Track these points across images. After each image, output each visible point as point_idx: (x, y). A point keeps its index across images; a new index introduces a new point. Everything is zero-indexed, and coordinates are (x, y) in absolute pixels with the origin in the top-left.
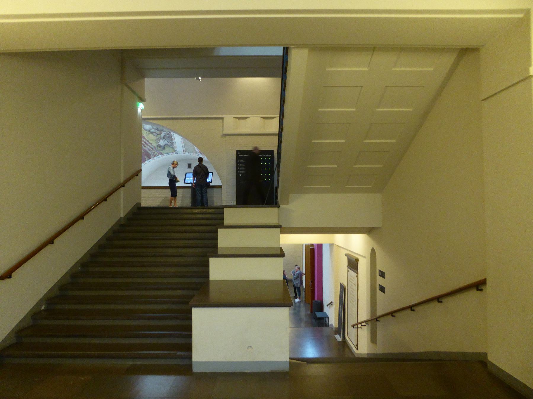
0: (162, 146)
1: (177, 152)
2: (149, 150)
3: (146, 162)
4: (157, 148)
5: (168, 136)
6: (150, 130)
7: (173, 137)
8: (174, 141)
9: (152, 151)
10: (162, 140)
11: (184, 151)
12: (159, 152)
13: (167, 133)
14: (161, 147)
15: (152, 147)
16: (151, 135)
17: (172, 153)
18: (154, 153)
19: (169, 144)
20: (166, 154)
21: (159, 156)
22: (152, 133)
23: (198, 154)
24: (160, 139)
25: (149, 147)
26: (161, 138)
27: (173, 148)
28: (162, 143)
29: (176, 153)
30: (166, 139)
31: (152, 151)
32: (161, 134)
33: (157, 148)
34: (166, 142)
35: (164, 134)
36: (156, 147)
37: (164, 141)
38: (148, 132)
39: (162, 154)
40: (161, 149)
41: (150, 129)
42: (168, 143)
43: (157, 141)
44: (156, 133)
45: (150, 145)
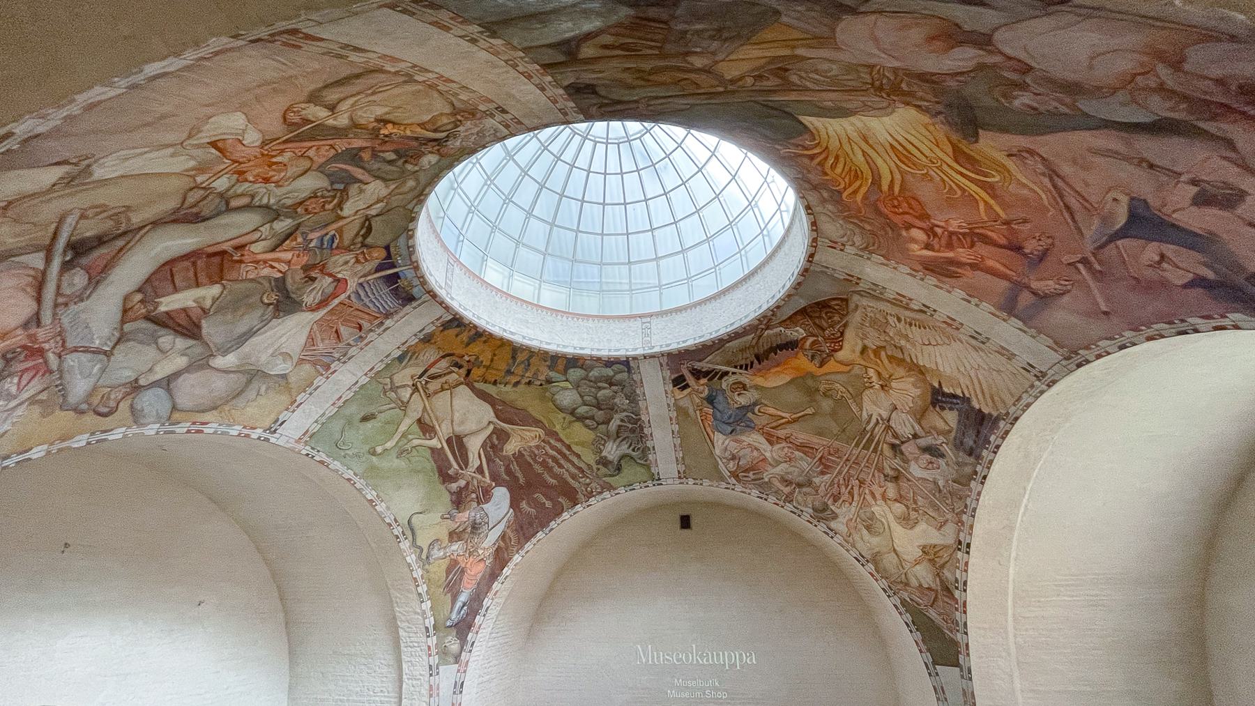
0: (611, 462)
1: (659, 479)
2: (574, 477)
3: (565, 515)
4: (598, 469)
5: (630, 426)
6: (575, 409)
7: (646, 431)
8: (649, 444)
9: (581, 480)
11: (682, 476)
12: (601, 483)
14: (610, 467)
15: (582, 465)
16: (578, 426)
17: (642, 485)
18: (588, 485)
20: (625, 486)
21: (602, 496)
22: (581, 419)
24: (605, 438)
25: (573, 470)
26: (608, 437)
27: (648, 467)
28: (612, 451)
29: (655, 482)
31: (581, 480)
32: (607, 422)
33: (598, 469)
34: (624, 449)
35: (619, 423)
36: (595, 467)
37: (617, 447)
38: (569, 418)
39: (611, 486)
42: (630, 451)
43: (597, 446)
44: (592, 418)
45: (575, 460)
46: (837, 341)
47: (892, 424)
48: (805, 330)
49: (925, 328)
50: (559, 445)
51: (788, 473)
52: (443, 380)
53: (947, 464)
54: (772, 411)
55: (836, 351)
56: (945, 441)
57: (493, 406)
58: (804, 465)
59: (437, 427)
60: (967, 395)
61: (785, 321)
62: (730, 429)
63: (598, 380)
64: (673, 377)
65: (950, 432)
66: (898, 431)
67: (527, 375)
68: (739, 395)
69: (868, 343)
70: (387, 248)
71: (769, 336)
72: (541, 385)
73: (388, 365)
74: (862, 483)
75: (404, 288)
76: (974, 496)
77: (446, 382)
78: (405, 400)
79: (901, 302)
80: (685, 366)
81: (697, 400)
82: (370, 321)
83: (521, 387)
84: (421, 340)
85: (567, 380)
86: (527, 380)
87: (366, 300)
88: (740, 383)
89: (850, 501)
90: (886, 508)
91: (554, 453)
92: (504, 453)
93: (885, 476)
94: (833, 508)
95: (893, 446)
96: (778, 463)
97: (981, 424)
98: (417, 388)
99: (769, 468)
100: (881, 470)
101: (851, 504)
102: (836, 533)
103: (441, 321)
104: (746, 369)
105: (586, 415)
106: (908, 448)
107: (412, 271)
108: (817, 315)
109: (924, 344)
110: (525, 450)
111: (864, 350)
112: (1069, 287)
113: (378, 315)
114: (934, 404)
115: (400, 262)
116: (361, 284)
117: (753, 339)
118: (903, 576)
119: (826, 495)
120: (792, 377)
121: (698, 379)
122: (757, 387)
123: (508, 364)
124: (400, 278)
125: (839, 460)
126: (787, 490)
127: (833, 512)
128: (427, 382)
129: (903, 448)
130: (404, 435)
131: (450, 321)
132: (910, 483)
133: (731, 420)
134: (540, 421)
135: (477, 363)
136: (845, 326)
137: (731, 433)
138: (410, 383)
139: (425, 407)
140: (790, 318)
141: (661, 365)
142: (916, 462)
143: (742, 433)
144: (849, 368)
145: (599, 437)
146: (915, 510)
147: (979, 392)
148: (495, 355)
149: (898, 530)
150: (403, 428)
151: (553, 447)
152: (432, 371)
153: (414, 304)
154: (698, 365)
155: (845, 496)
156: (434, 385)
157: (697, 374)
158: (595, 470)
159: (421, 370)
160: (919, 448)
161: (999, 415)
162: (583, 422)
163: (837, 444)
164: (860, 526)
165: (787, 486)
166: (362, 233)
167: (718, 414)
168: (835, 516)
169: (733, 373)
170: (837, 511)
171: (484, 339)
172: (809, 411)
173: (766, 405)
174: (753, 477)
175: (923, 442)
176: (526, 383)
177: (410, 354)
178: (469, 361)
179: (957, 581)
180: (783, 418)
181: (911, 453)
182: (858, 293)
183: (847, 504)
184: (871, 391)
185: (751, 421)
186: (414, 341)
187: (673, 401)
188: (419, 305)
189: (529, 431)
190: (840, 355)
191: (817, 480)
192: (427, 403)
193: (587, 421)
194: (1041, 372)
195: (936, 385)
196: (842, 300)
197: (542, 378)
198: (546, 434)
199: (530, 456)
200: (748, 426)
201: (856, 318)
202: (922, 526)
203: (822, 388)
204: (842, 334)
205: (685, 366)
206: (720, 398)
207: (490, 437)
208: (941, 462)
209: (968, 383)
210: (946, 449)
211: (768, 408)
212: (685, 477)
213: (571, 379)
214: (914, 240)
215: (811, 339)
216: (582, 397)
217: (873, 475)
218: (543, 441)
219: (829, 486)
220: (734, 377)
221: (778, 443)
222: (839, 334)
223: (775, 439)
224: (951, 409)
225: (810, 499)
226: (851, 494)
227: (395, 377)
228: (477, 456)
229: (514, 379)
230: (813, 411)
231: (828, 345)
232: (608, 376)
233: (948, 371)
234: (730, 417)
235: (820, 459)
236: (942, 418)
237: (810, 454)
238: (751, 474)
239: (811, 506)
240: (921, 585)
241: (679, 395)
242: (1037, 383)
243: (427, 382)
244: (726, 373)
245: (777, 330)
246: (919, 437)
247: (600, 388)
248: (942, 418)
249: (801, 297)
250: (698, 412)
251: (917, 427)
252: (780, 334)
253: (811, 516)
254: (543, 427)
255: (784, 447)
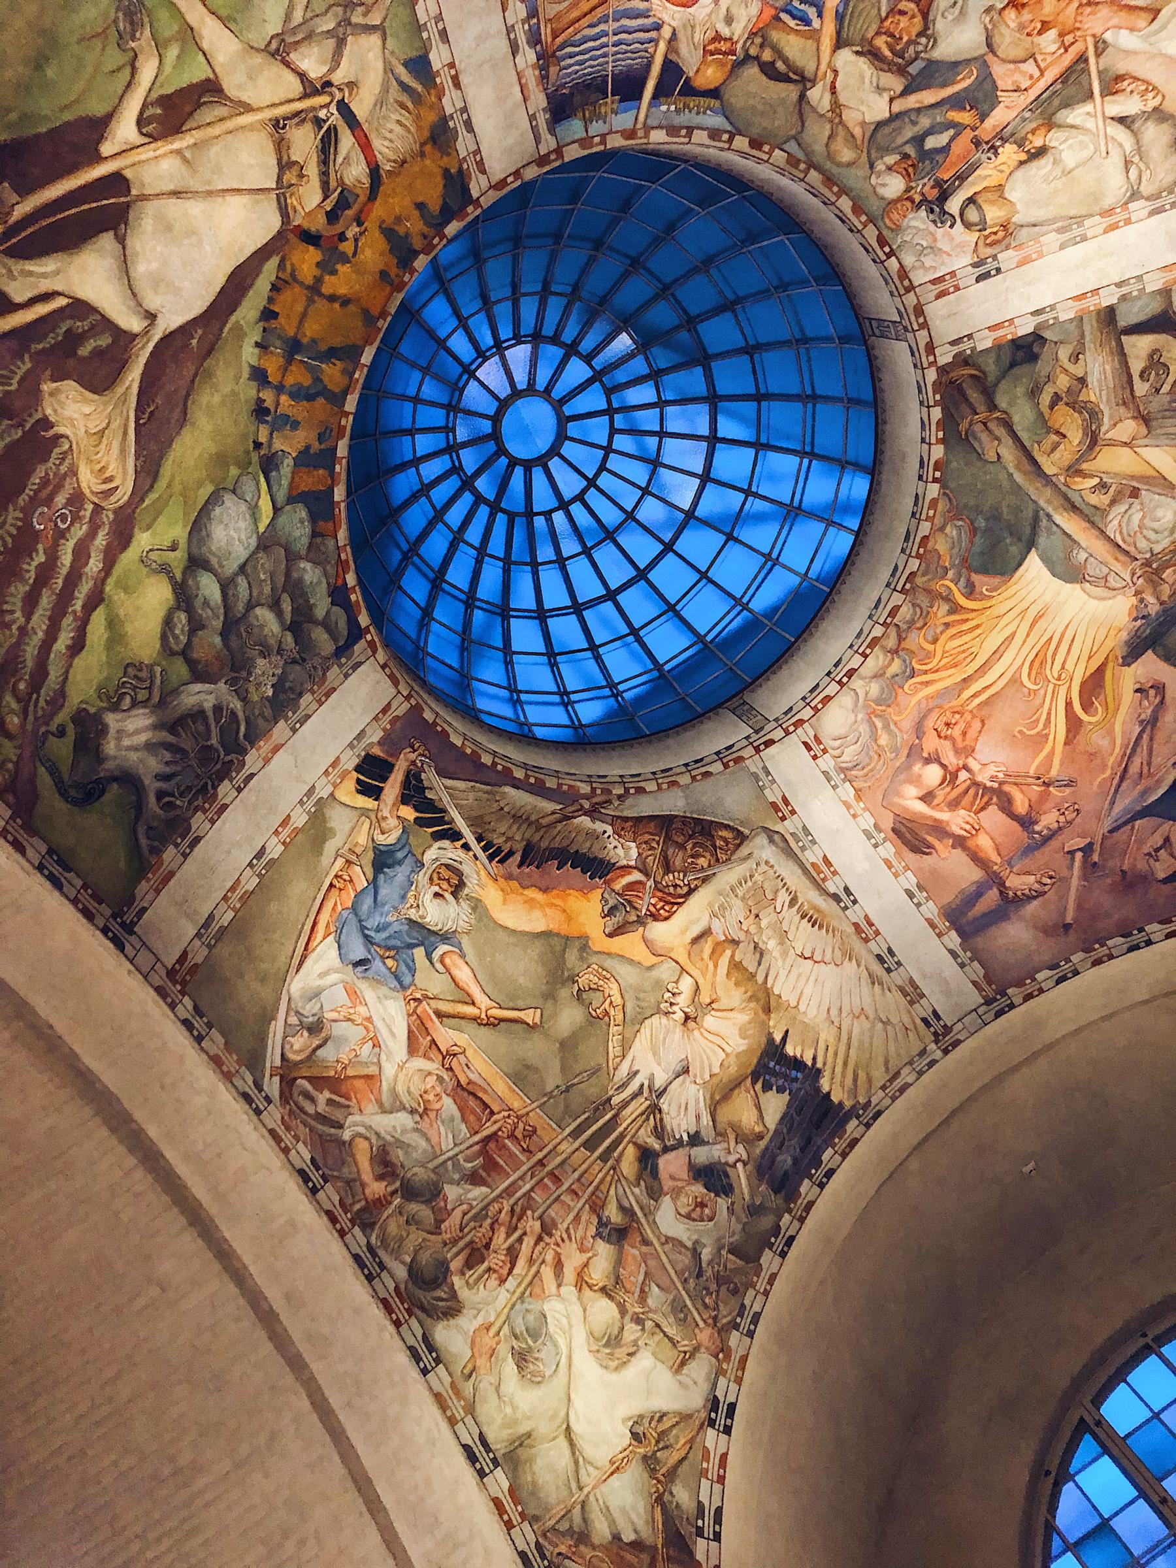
0: (100, 758)
1: (129, 928)
5: (214, 741)
6: (206, 565)
7: (225, 788)
8: (198, 821)
10: (156, 727)
13: (233, 714)
15: (54, 673)
19: (152, 799)
20: (51, 852)
22: (184, 596)
23: (259, 1086)
26: (162, 703)
29: (115, 926)
30: (168, 747)
32: (200, 674)
33: (61, 733)
34: (150, 766)
35: (209, 703)
37: (149, 747)
38: (177, 559)
40: (65, 770)
41: (214, 561)
42: (152, 786)
44: (196, 626)
46: (673, 900)
47: (664, 1104)
48: (639, 854)
49: (821, 927)
50: (94, 565)
51: (400, 1144)
52: (312, 171)
53: (731, 1210)
54: (463, 974)
55: (655, 917)
56: (745, 1157)
57: (194, 322)
58: (447, 1142)
59: (176, 145)
60: (819, 1065)
61: (626, 819)
62: (358, 951)
63: (294, 587)
64: (377, 751)
65: (760, 1137)
66: (666, 1119)
67: (284, 399)
68: (437, 895)
69: (717, 927)
70: (714, 93)
71: (579, 830)
72: (258, 445)
73: (419, 28)
74: (547, 1229)
75: (594, 103)
76: (761, 1285)
77: (301, 176)
78: (293, 56)
79: (819, 872)
80: (413, 756)
81: (362, 839)
82: (558, 16)
83: (250, 391)
84: (444, 119)
85: (276, 510)
86: (269, 403)
87: (612, 26)
88: (459, 874)
89: (505, 1272)
90: (577, 1309)
91: (66, 559)
92: (47, 387)
93: (601, 1224)
94: (457, 1281)
95: (647, 1157)
96: (397, 1106)
97: (818, 1127)
98: (316, 92)
99: (370, 1108)
100: (597, 1207)
101: (503, 1281)
102: (438, 1361)
103: (473, 168)
104: (491, 858)
105: (198, 603)
106: (672, 1165)
107: (629, 125)
108: (680, 839)
109: (802, 956)
110: (63, 457)
111: (706, 933)
112: (1046, 888)
113: (559, 40)
114: (755, 1076)
115: (664, 108)
116: (658, 27)
117: (553, 813)
118: (577, 1511)
119: (455, 1242)
120: (551, 926)
121: (405, 800)
122: (477, 905)
123: (314, 341)
124: (621, 101)
125: (522, 1157)
126: (377, 1188)
127: (454, 1295)
128: (318, 123)
129: (662, 1162)
130: (189, 35)
131: (466, 190)
132: (644, 1249)
133: (379, 937)
134: (155, 476)
135: (332, 260)
136: (705, 880)
137: (357, 964)
138: (338, 77)
139: (248, 108)
140: (639, 820)
141: (384, 711)
142: (674, 1200)
143: (378, 981)
144: (655, 960)
145: (152, 678)
146: (638, 1320)
147: (840, 1061)
148: (345, 302)
149: (586, 1366)
150: (212, 33)
151: (81, 553)
152: (347, 141)
153: (542, 120)
154: (430, 776)
155: (496, 1259)
156: (303, 142)
157: (413, 792)
158: (53, 728)
159: (361, 107)
160: (691, 1166)
161: (853, 1107)
162: (178, 608)
163: (537, 1118)
164: (504, 1350)
165: (380, 1178)
166: (780, 65)
167: (368, 901)
168: (452, 1309)
169: (466, 847)
170: (463, 1293)
171: (394, 271)
172: (529, 1016)
173: (463, 956)
174: (322, 1107)
175: (701, 1155)
176: (260, 401)
177: (420, 88)
178: (342, 237)
179: (700, 1507)
180: (473, 1004)
181: (672, 1178)
182: (770, 834)
183: (493, 1282)
184: (664, 1020)
185: (412, 971)
186: (450, 102)
187: (325, 794)
188: (535, 130)
189: (123, 451)
190: (659, 931)
191: (452, 1192)
192: (259, 116)
193: (183, 616)
194: (945, 1026)
195: (778, 1038)
196: (739, 833)
197: (278, 445)
198: (115, 512)
199: (45, 481)
200: (397, 978)
201: (728, 876)
202: (645, 1361)
203: (583, 981)
204: (691, 891)
205: (413, 756)
206: (401, 873)
207: (107, 324)
208: (722, 1203)
209: (831, 1040)
210: (741, 1177)
211: (460, 962)
212: (184, 983)
213: (282, 520)
214: (916, 781)
215: (636, 876)
216: (242, 569)
217: (577, 1218)
218: (98, 509)
219: (475, 1218)
220: (460, 854)
221: (425, 1056)
222: (686, 889)
223: (425, 1042)
224: (780, 1090)
225: (416, 1237)
226: (513, 1255)
227: (375, 40)
228: (45, 286)
229: (272, 366)
230: (537, 1020)
231: (653, 901)
232: (311, 607)
233: (812, 1012)
234: (378, 930)
235: (488, 1139)
236: (758, 1107)
237: (472, 1118)
238: (323, 1097)
239: (408, 1259)
240: (617, 1537)
241: (348, 793)
242: (933, 1046)
243: (318, 123)
244: (455, 836)
245: (599, 826)
246: (704, 1143)
247: (275, 606)
248: (758, 1107)
249: (686, 797)
250: (340, 862)
251: (706, 1119)
252: (595, 836)
253: (397, 1288)
254: (139, 494)
255: (430, 1074)
